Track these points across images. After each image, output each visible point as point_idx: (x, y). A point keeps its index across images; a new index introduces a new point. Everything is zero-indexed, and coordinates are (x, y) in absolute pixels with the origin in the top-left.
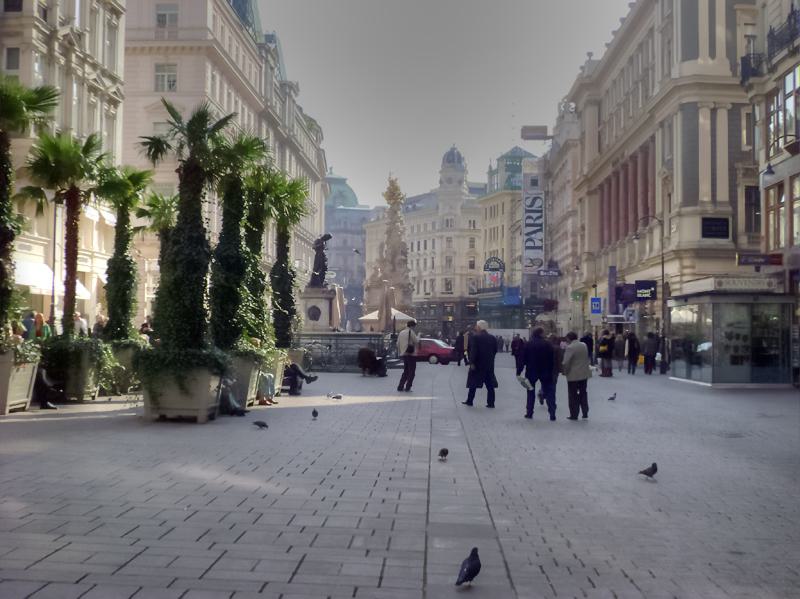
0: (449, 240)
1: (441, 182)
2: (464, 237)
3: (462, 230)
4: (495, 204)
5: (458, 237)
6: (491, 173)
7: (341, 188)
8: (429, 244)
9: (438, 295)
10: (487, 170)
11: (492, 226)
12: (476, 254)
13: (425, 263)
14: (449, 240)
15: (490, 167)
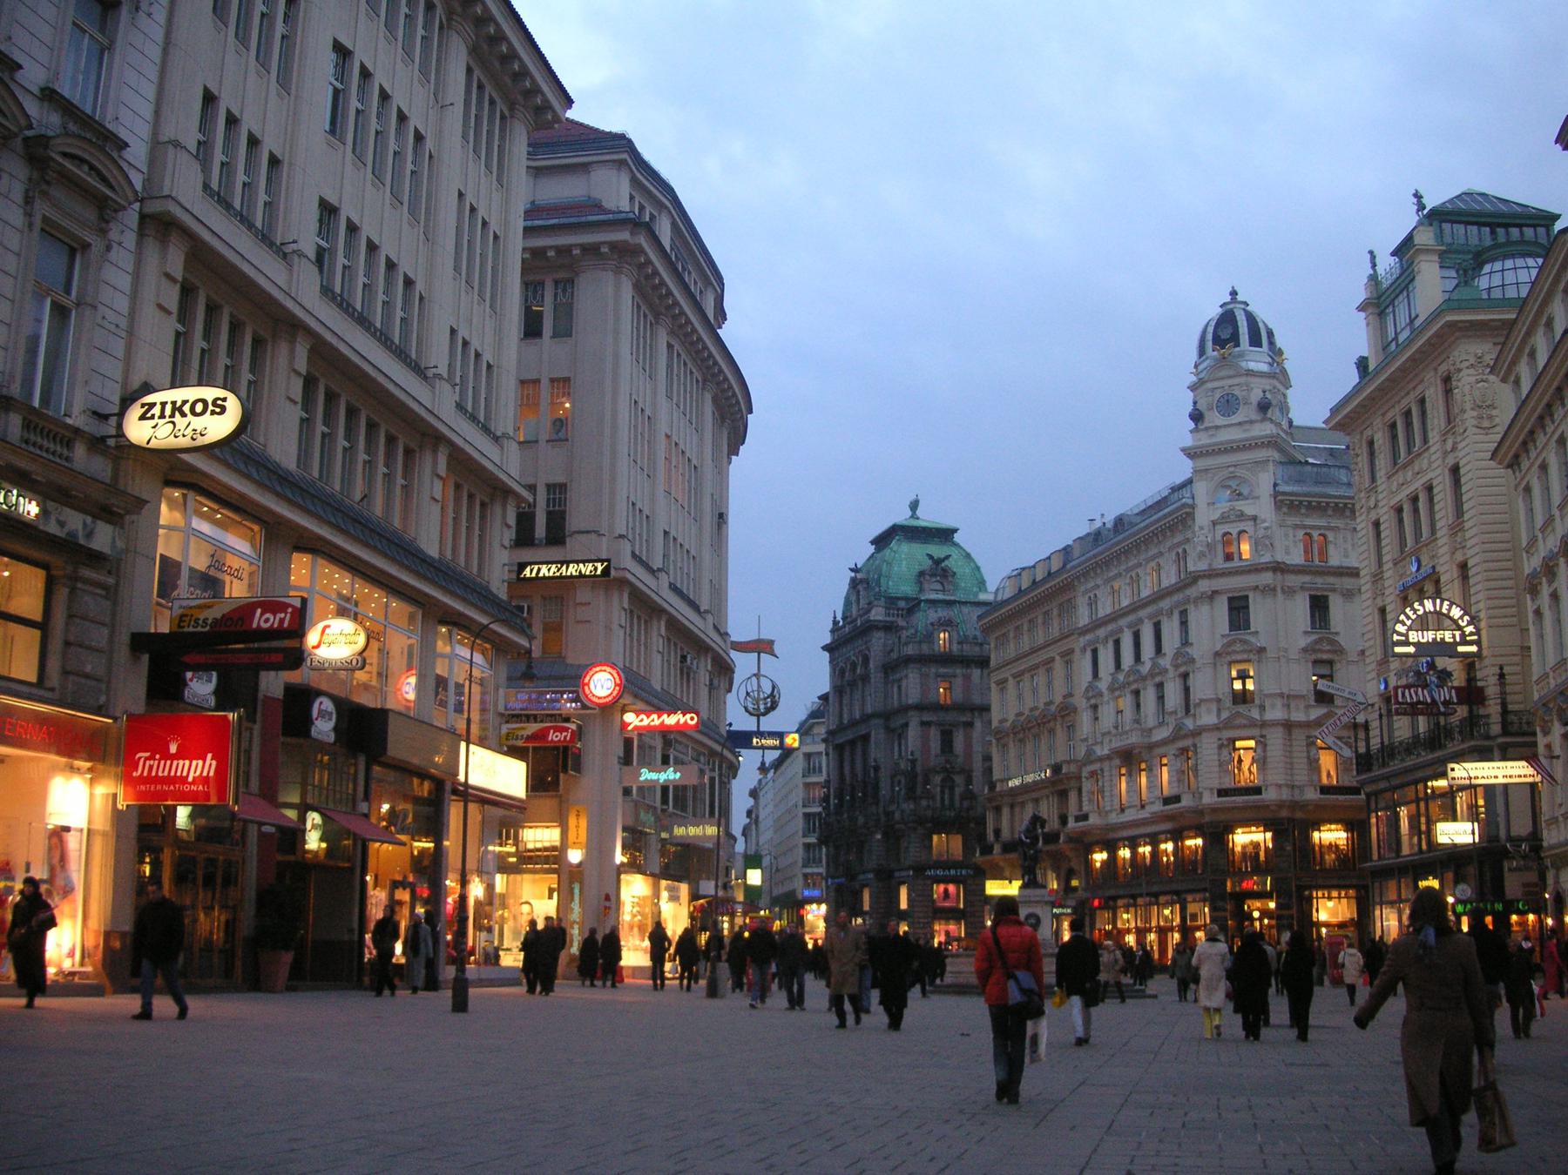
0: (1239, 609)
1: (1197, 417)
2: (1290, 592)
3: (1279, 568)
4: (1410, 401)
5: (1269, 590)
6: (1381, 301)
7: (938, 551)
8: (1171, 630)
9: (1209, 799)
10: (1361, 295)
11: (1403, 495)
12: (1340, 651)
13: (1161, 698)
14: (1239, 609)
15: (1373, 278)
